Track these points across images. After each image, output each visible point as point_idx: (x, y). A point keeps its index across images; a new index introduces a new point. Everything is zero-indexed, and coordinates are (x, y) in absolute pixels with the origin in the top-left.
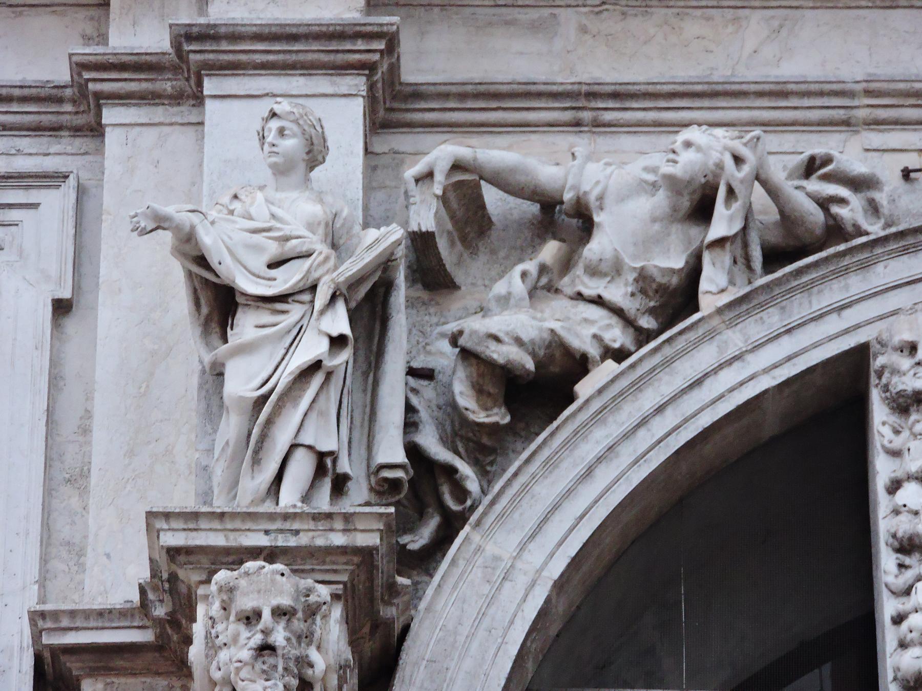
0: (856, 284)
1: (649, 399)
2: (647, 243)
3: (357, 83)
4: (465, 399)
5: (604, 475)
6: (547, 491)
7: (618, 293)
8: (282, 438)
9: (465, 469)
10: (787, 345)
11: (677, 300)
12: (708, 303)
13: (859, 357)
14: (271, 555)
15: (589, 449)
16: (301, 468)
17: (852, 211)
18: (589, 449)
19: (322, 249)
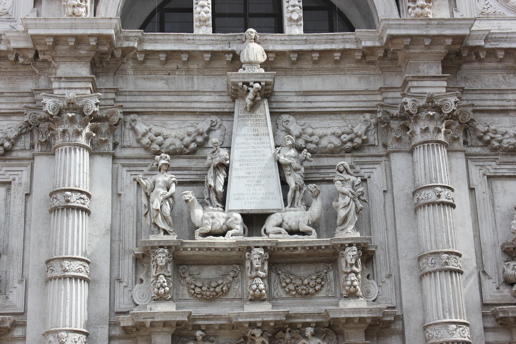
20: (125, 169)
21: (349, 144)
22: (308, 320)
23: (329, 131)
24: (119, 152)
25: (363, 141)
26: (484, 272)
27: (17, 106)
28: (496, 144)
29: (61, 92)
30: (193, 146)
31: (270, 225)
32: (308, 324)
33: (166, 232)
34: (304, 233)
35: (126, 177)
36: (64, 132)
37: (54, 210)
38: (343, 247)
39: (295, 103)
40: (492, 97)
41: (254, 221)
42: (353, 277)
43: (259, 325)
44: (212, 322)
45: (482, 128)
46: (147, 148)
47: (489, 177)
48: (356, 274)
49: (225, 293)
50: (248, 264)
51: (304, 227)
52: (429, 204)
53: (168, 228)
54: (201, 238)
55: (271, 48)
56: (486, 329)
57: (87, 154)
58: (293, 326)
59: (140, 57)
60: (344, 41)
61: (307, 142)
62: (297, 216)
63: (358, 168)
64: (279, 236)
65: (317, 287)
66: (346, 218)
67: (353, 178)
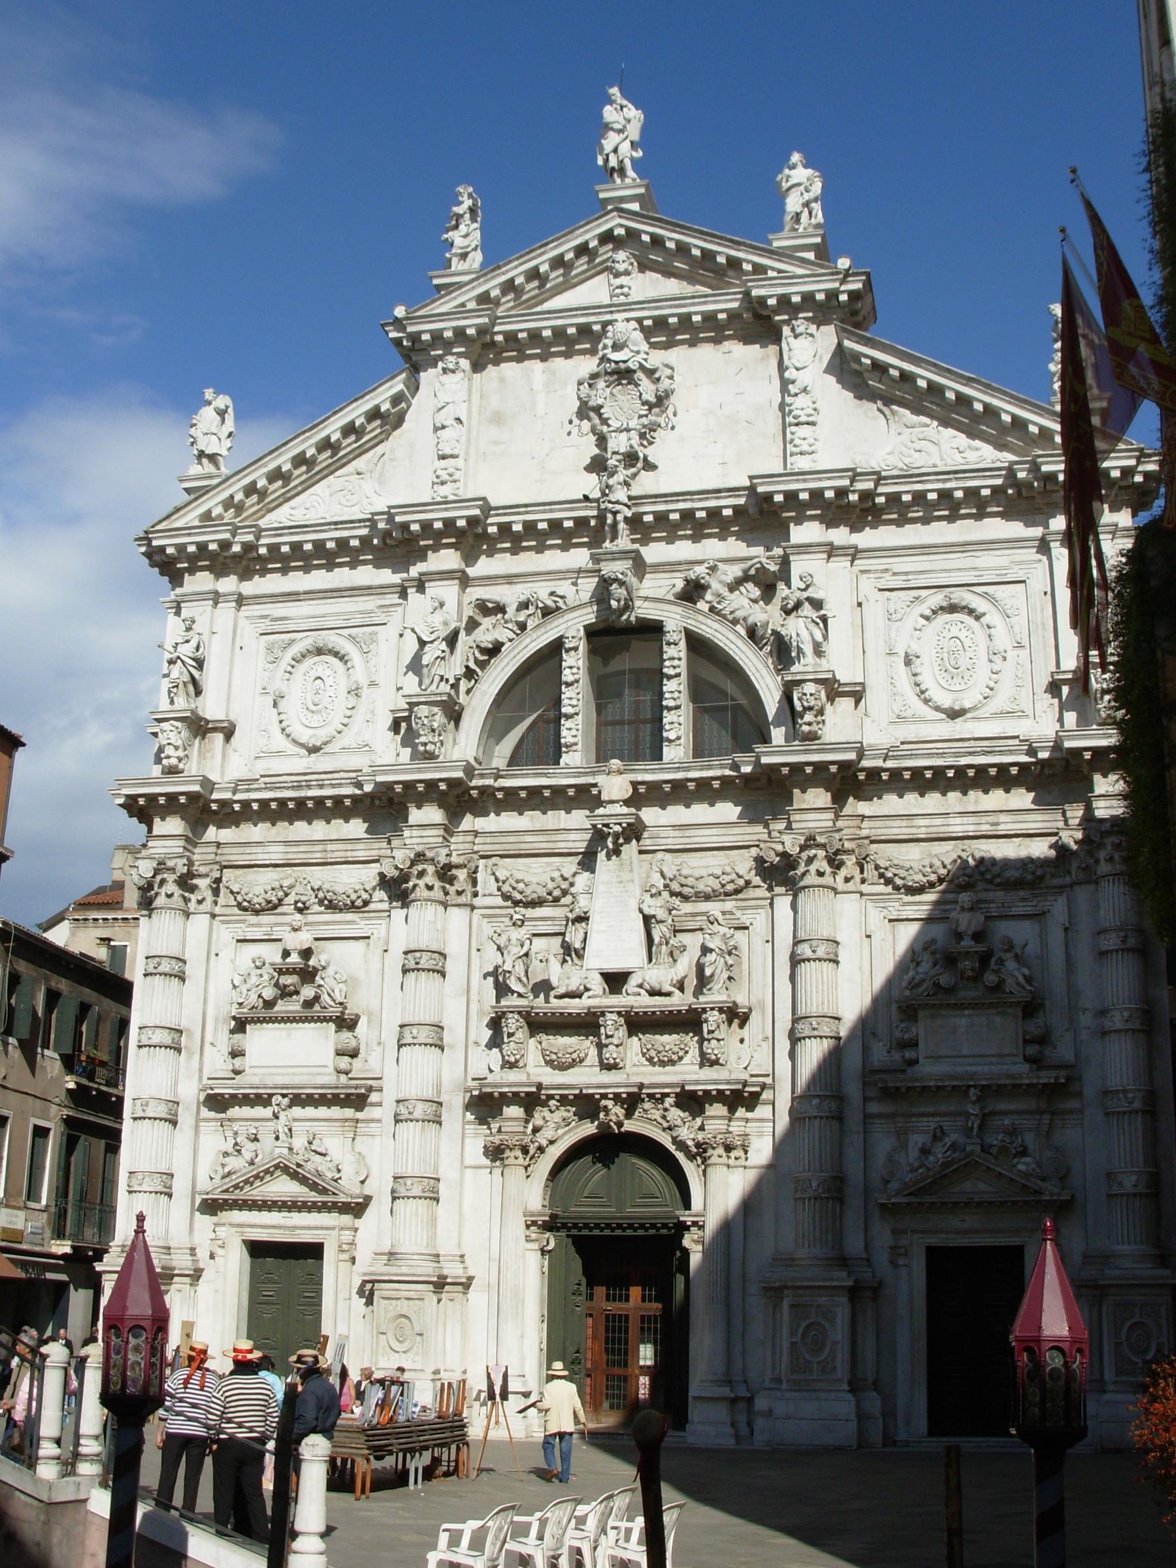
0: (561, 620)
1: (516, 651)
2: (515, 616)
3: (457, 581)
4: (478, 655)
5: (507, 669)
6: (494, 674)
7: (510, 626)
8: (433, 672)
9: (478, 670)
10: (545, 636)
11: (523, 627)
12: (529, 628)
13: (562, 637)
14: (426, 703)
15: (503, 664)
16: (437, 679)
17: (561, 604)
18: (503, 664)
19: (441, 627)
20: (486, 920)
21: (730, 887)
22: (667, 1090)
23: (704, 873)
24: (477, 902)
25: (748, 883)
26: (874, 1034)
27: (375, 853)
28: (899, 882)
29: (414, 841)
30: (557, 893)
31: (631, 984)
32: (668, 1095)
33: (520, 995)
34: (668, 994)
35: (488, 929)
36: (415, 886)
37: (405, 971)
38: (704, 1010)
39: (673, 839)
40: (898, 823)
41: (615, 981)
42: (714, 1042)
43: (611, 1096)
44: (566, 1092)
45: (882, 863)
46: (506, 897)
47: (890, 921)
48: (718, 1040)
49: (581, 1061)
50: (602, 1030)
51: (667, 988)
52: (804, 961)
53: (521, 990)
54: (556, 1000)
55: (640, 777)
56: (866, 1100)
57: (441, 908)
58: (651, 1096)
59: (500, 795)
60: (722, 767)
61: (682, 886)
62: (661, 975)
63: (738, 914)
64: (638, 998)
65: (681, 1054)
66: (712, 975)
67: (723, 930)
